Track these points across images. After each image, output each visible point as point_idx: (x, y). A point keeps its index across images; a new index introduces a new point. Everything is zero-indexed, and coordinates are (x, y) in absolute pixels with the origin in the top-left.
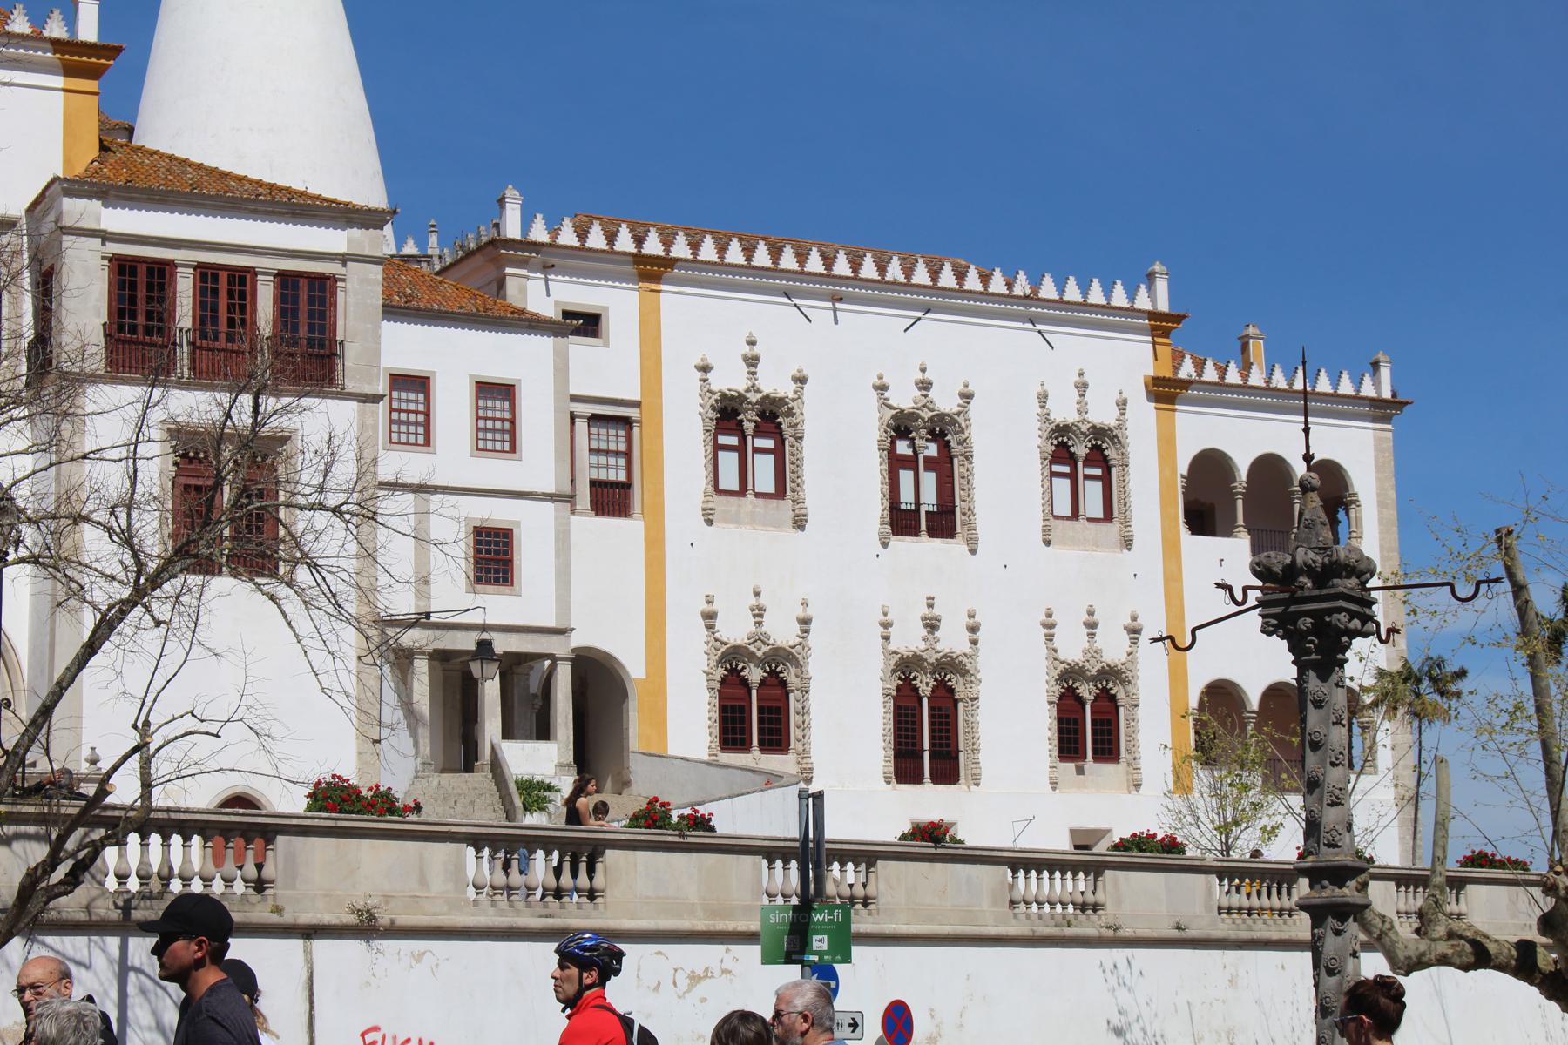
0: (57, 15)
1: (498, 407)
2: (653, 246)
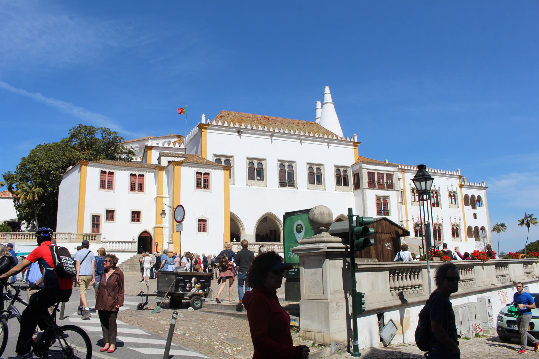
2: (403, 167)
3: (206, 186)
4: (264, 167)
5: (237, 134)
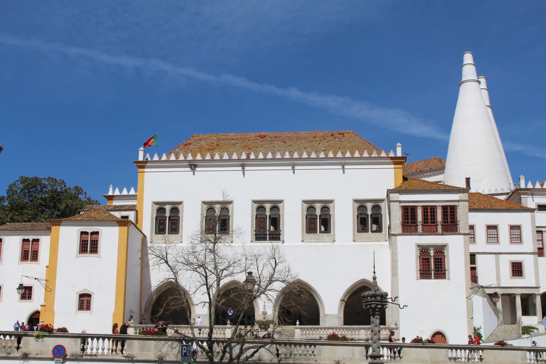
0: (392, 151)
1: (516, 232)
3: (94, 249)
4: (230, 214)
5: (189, 169)
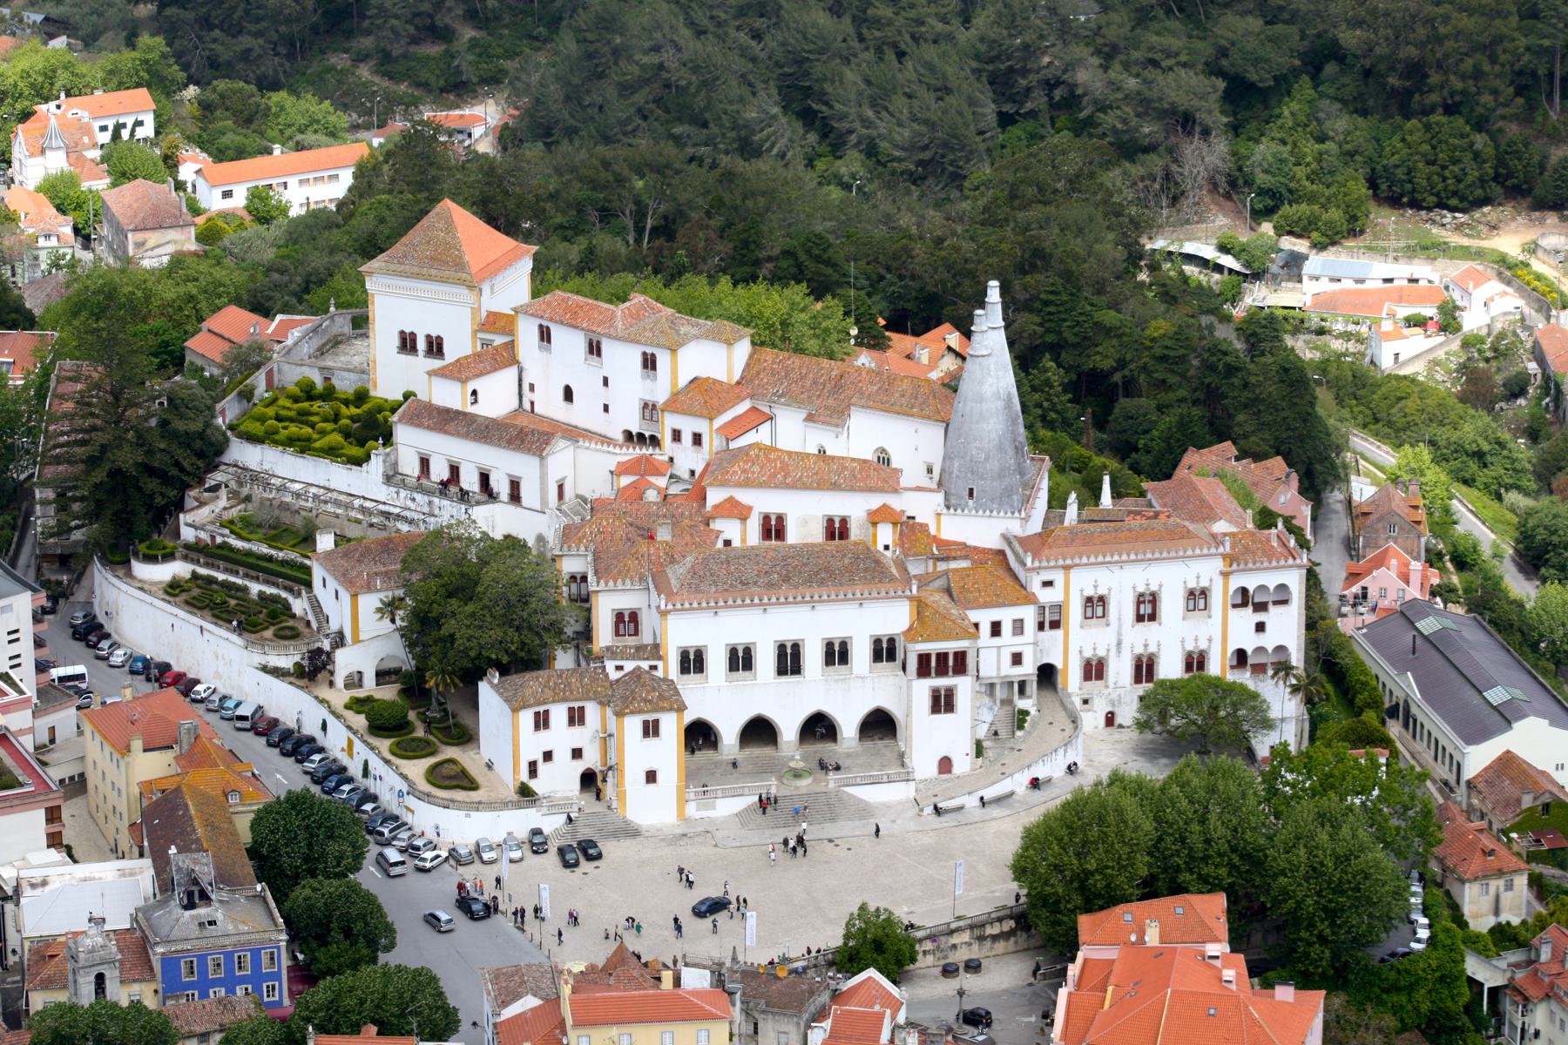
2: (1069, 562)
